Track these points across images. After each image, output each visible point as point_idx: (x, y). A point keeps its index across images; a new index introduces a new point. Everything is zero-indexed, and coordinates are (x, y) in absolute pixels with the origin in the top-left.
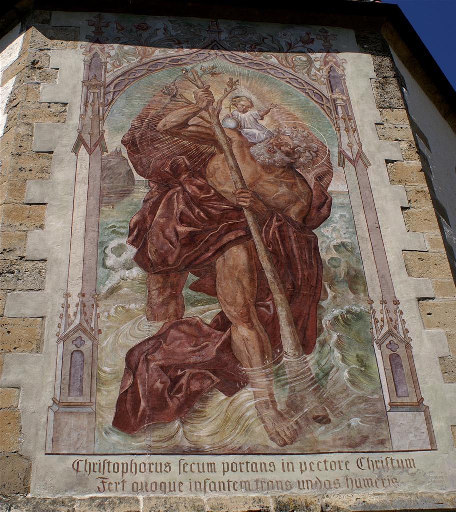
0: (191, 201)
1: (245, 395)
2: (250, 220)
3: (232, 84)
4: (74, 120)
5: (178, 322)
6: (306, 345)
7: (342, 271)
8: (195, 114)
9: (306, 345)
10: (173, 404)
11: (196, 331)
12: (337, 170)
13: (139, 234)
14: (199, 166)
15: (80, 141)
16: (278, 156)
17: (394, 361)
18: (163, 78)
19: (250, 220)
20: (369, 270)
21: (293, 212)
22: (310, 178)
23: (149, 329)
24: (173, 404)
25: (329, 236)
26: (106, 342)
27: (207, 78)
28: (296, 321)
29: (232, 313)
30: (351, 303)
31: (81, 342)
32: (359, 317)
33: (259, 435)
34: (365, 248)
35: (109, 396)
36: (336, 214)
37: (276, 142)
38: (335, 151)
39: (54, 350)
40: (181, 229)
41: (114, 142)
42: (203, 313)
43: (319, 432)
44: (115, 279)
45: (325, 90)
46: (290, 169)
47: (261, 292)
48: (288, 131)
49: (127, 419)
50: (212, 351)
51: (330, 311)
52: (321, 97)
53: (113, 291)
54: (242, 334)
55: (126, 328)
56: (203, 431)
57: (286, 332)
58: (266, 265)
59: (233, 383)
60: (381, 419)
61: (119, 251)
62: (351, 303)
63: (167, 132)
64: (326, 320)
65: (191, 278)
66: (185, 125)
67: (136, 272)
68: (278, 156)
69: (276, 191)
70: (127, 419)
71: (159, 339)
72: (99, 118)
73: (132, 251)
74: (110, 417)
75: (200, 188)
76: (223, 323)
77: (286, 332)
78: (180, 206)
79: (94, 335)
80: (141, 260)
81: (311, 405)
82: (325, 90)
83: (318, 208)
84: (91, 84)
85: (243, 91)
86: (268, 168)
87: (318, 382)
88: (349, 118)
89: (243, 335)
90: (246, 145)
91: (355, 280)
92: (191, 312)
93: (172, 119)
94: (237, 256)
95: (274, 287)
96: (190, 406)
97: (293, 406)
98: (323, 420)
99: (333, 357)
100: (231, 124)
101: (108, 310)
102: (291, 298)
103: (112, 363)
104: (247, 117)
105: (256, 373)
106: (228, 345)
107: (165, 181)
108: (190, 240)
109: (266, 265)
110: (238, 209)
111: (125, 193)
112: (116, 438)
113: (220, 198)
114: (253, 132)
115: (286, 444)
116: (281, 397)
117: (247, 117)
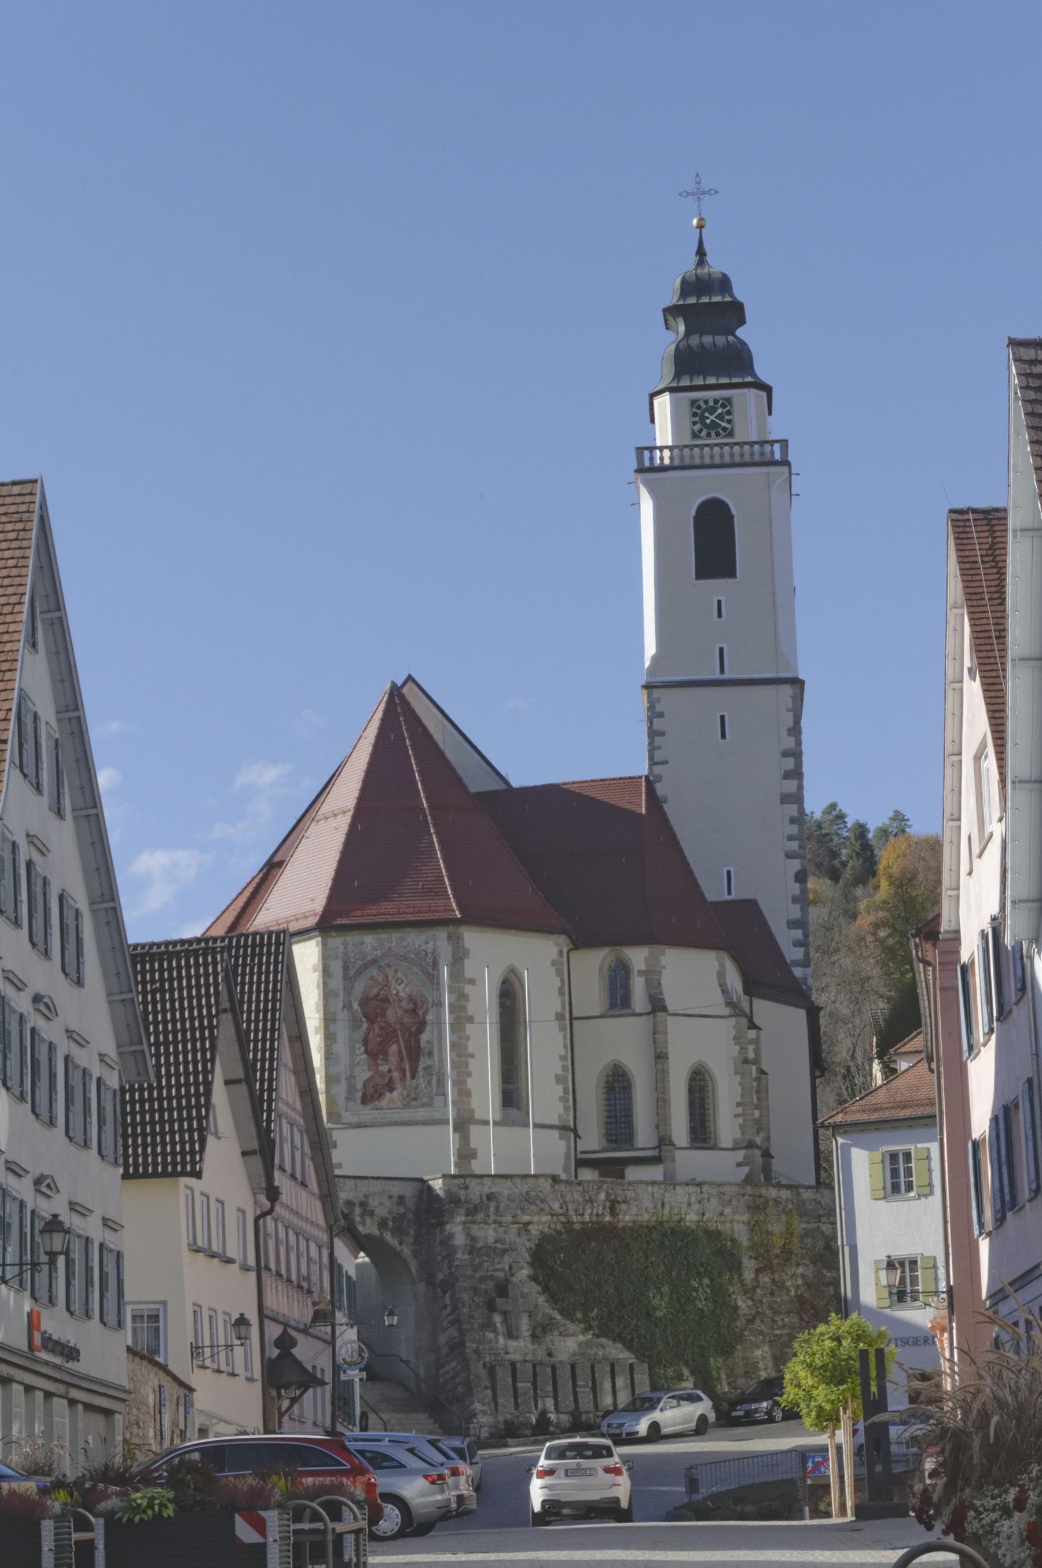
0: (381, 1028)
1: (395, 1094)
2: (399, 1034)
3: (396, 971)
4: (341, 997)
5: (377, 1072)
6: (413, 1077)
7: (426, 1051)
8: (382, 989)
9: (413, 1077)
10: (376, 1096)
11: (382, 1075)
12: (431, 1010)
13: (365, 1042)
14: (384, 1016)
15: (344, 1006)
16: (411, 1006)
17: (439, 1081)
18: (373, 971)
19: (399, 1034)
20: (436, 1050)
21: (413, 1029)
22: (421, 1014)
23: (367, 1075)
24: (376, 1096)
25: (424, 1037)
26: (357, 1079)
27: (387, 969)
28: (411, 1070)
29: (393, 1067)
30: (429, 1062)
31: (351, 1078)
32: (430, 1067)
33: (399, 1104)
34: (436, 1042)
35: (359, 1095)
36: (428, 1028)
37: (411, 999)
38: (430, 1000)
39: (344, 1084)
40: (378, 1039)
41: (356, 1005)
42: (384, 1068)
43: (414, 1103)
44: (358, 1060)
45: (430, 969)
46: (414, 1011)
47: (402, 1060)
48: (415, 993)
49: (364, 1101)
50: (386, 1081)
51: (422, 1065)
52: (429, 974)
53: (358, 1064)
54: (396, 1075)
55: (363, 1074)
56: (383, 1103)
57: (408, 1073)
58: (404, 1050)
59: (391, 1089)
60: (432, 1099)
61: (359, 1049)
62: (429, 1062)
63: (372, 999)
64: (420, 1068)
65: (381, 1056)
66: (378, 994)
67: (365, 1056)
68: (411, 1006)
69: (408, 1020)
70: (364, 1101)
71: (372, 1077)
72: (350, 994)
73: (363, 1049)
74: (359, 1101)
75: (385, 1022)
76: (390, 1071)
77: (408, 1073)
78: (377, 1030)
79: (354, 1077)
80: (366, 1052)
81: (413, 1095)
82: (430, 969)
83: (422, 1026)
84: (346, 977)
85: (400, 975)
86: (406, 1011)
87: (416, 1088)
88: (438, 984)
89: (396, 1075)
90: (400, 1001)
91: (430, 1054)
92: (381, 1068)
93: (375, 992)
94: (395, 1047)
95: (405, 1058)
96: (380, 1096)
97: (408, 1096)
98: (415, 1099)
99: (421, 1080)
100: (395, 992)
101: (357, 1069)
102: (410, 1061)
103: (359, 1085)
104: (400, 988)
105: (399, 1086)
106: (391, 1079)
107: (371, 1021)
108: (380, 1044)
109: (404, 1050)
110: (395, 1030)
111: (360, 1027)
112: (361, 1106)
113: (390, 1025)
114: (402, 994)
115: (405, 1107)
116: (405, 1093)
117: (400, 988)
